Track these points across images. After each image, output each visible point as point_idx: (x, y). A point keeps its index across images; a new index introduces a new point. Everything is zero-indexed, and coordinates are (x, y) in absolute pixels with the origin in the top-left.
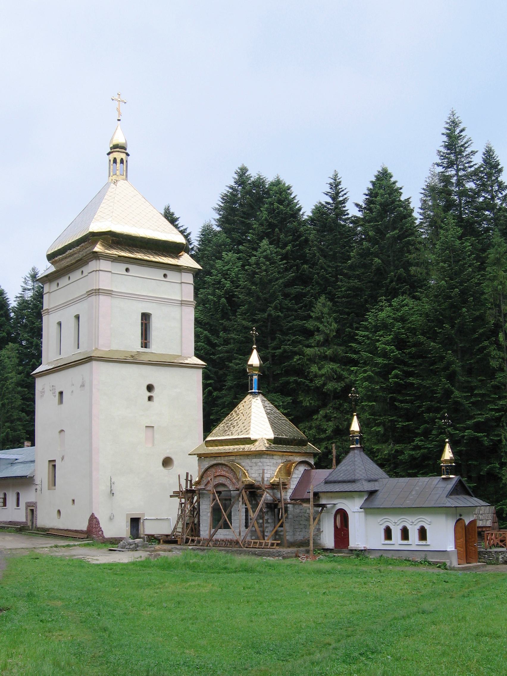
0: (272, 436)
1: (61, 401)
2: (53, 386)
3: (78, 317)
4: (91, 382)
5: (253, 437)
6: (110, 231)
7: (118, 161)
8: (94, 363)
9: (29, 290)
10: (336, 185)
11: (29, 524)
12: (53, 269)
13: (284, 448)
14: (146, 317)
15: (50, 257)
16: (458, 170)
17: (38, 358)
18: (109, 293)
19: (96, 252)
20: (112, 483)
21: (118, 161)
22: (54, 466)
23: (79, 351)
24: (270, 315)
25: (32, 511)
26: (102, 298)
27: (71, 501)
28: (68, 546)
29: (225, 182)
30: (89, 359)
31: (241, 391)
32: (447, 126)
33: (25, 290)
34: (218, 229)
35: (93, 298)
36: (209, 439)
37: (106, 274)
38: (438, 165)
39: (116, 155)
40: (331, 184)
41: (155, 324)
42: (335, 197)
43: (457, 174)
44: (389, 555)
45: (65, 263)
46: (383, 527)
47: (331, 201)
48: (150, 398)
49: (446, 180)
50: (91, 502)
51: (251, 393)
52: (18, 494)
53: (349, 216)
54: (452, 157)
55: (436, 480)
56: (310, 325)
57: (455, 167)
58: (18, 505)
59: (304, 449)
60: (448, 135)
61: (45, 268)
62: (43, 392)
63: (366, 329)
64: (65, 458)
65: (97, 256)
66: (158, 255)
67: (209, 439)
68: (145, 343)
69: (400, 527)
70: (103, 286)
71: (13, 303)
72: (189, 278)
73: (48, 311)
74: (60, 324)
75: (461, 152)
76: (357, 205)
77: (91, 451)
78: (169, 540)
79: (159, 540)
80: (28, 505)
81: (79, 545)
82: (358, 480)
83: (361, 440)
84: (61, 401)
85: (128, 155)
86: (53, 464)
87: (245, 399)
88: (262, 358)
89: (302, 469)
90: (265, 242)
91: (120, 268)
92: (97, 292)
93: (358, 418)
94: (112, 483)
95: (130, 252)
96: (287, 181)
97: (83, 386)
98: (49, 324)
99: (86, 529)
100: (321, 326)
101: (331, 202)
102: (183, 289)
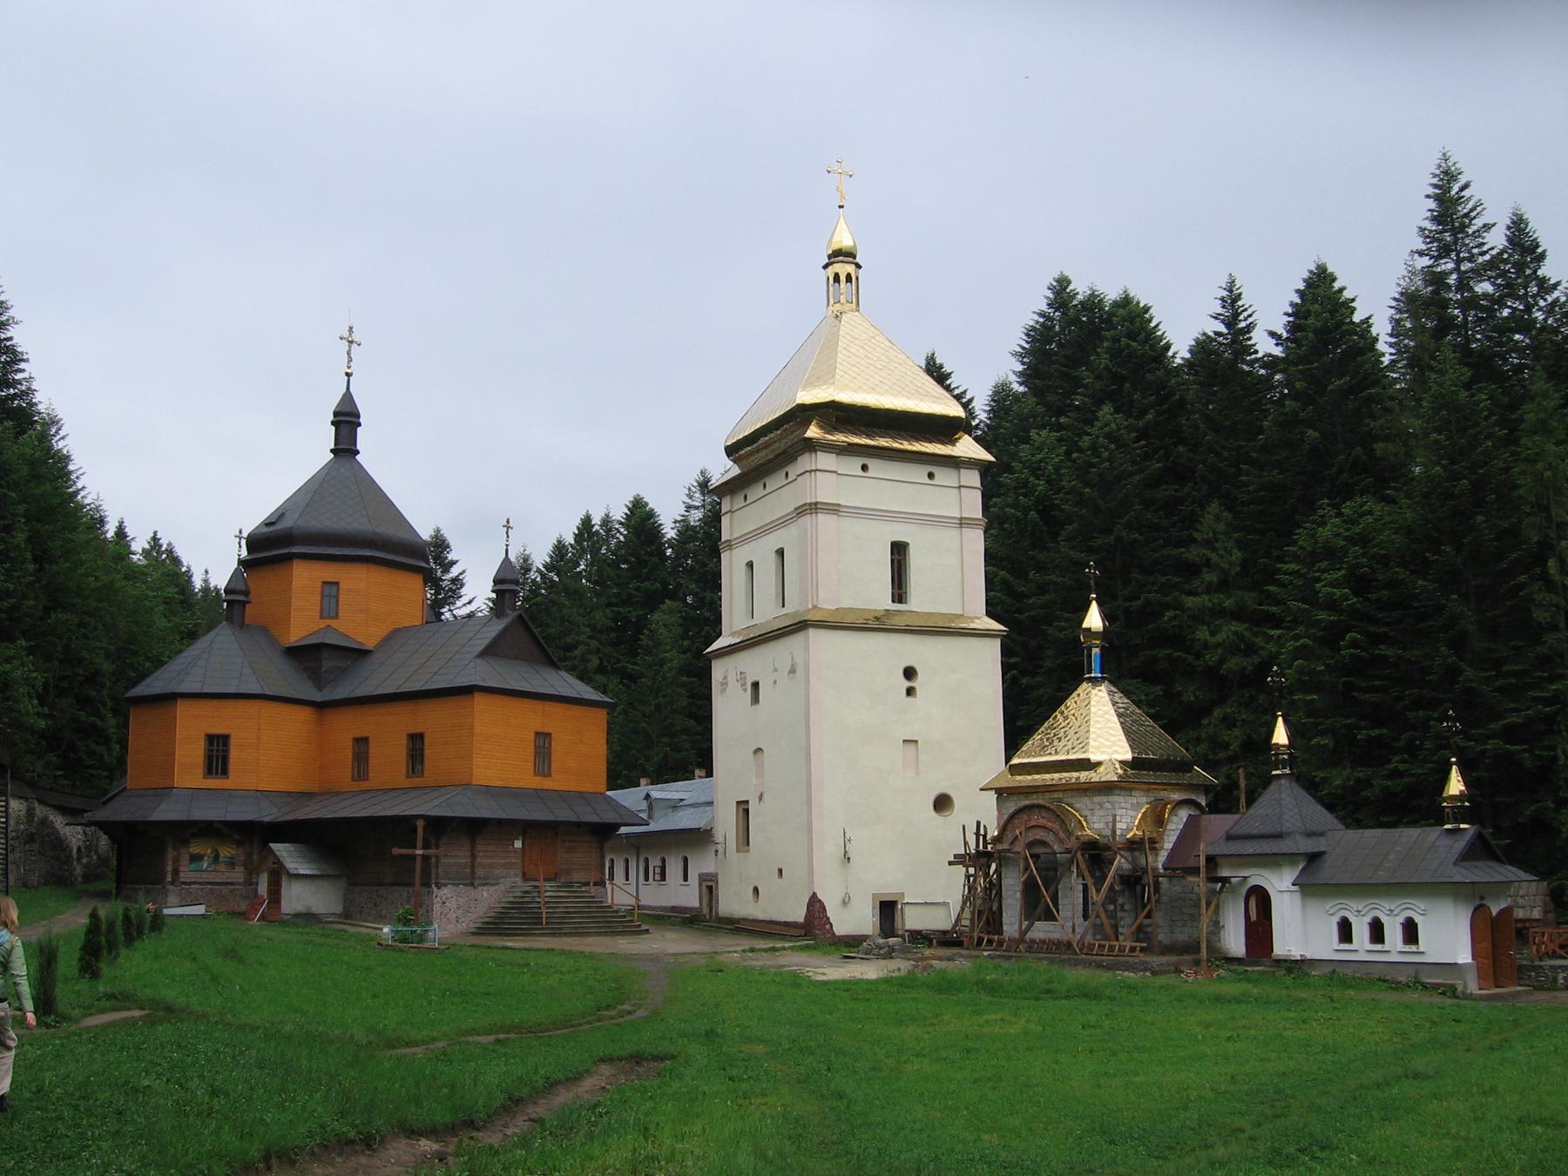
0: (1128, 756)
1: (755, 699)
3: (780, 553)
4: (807, 664)
5: (1094, 758)
6: (833, 402)
7: (843, 278)
8: (812, 632)
9: (697, 508)
10: (1232, 300)
11: (706, 910)
12: (736, 471)
13: (1149, 776)
14: (899, 551)
15: (731, 451)
16: (1459, 262)
17: (714, 627)
18: (834, 509)
19: (810, 439)
20: (847, 841)
21: (843, 278)
22: (747, 811)
23: (785, 611)
24: (1119, 539)
25: (710, 888)
26: (822, 518)
28: (774, 949)
29: (1032, 304)
30: (801, 626)
31: (1071, 677)
32: (1435, 181)
33: (689, 508)
34: (1022, 389)
35: (807, 520)
36: (1015, 761)
37: (828, 476)
38: (1421, 254)
39: (837, 268)
40: (1222, 299)
41: (916, 562)
42: (1231, 322)
43: (1457, 269)
44: (1349, 971)
45: (756, 460)
46: (1336, 919)
47: (1223, 329)
48: (910, 692)
49: (1435, 279)
50: (811, 874)
51: (1090, 680)
52: (686, 860)
53: (1260, 355)
54: (1448, 237)
55: (1433, 833)
56: (1193, 554)
57: (1453, 255)
58: (686, 879)
59: (1186, 778)
60: (1438, 199)
61: (722, 469)
62: (724, 684)
63: (1296, 558)
64: (765, 797)
65: (811, 446)
66: (917, 440)
67: (1015, 761)
68: (899, 593)
69: (1368, 919)
70: (824, 497)
71: (670, 532)
72: (973, 478)
73: (730, 545)
74: (750, 565)
75: (1463, 227)
76: (1272, 334)
77: (809, 785)
78: (947, 940)
79: (931, 941)
80: (703, 878)
81: (792, 948)
82: (1288, 834)
83: (1291, 762)
84: (755, 699)
85: (858, 266)
86: (743, 807)
87: (1079, 690)
88: (1105, 616)
89: (1184, 814)
90: (1106, 410)
91: (852, 465)
92: (814, 508)
93: (1285, 721)
94: (847, 841)
95: (869, 436)
96: (1142, 297)
97: (793, 671)
98: (732, 566)
99: (801, 920)
100: (1213, 556)
101: (1225, 331)
102: (961, 497)
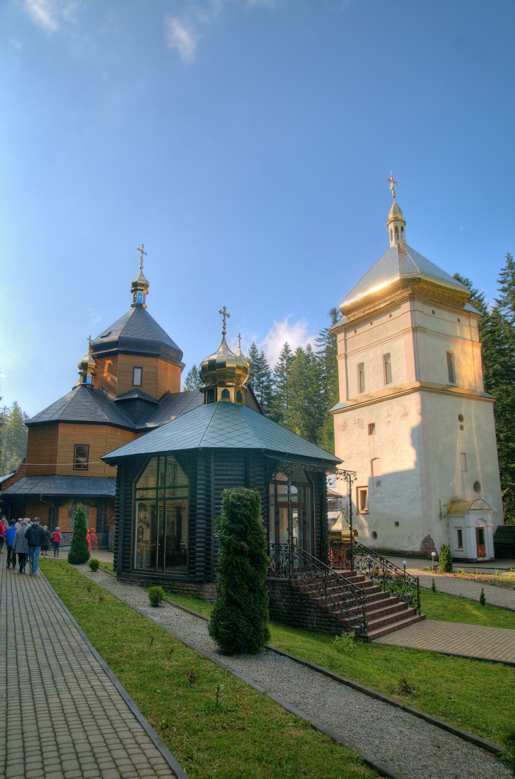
2: (359, 419)
3: (387, 357)
18: (424, 330)
26: (419, 334)
27: (393, 524)
62: (344, 426)
70: (419, 323)
74: (361, 366)
